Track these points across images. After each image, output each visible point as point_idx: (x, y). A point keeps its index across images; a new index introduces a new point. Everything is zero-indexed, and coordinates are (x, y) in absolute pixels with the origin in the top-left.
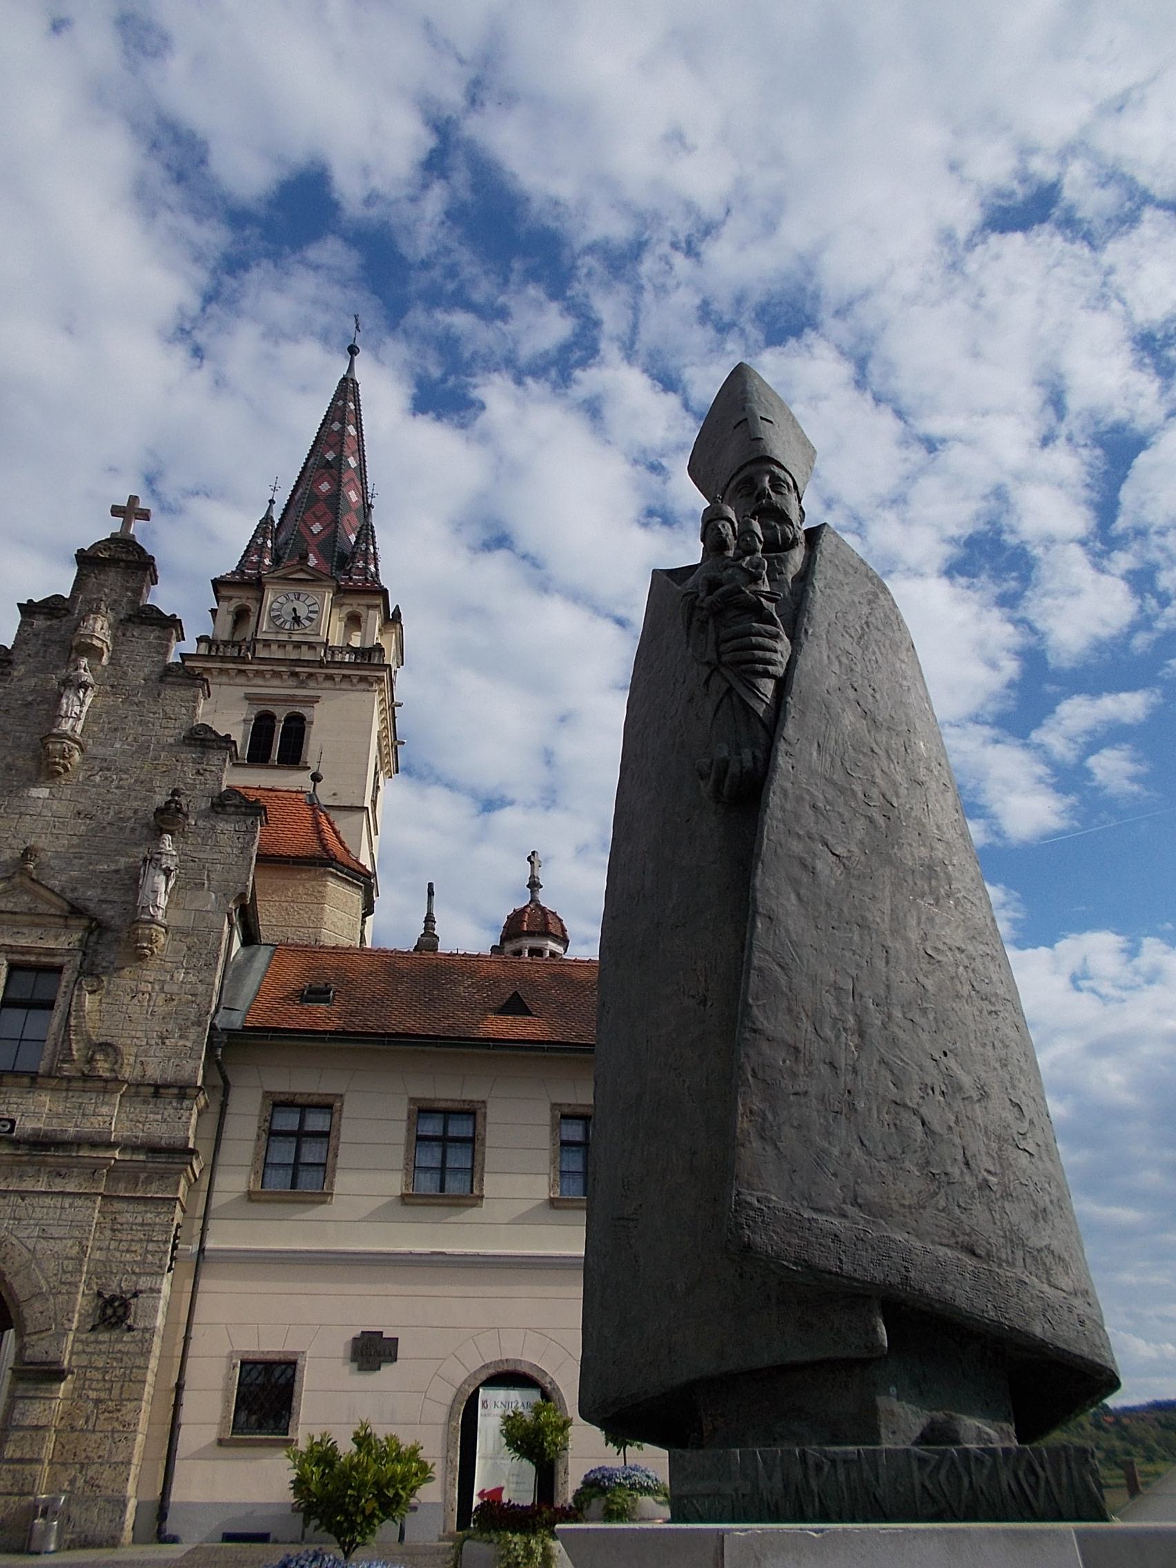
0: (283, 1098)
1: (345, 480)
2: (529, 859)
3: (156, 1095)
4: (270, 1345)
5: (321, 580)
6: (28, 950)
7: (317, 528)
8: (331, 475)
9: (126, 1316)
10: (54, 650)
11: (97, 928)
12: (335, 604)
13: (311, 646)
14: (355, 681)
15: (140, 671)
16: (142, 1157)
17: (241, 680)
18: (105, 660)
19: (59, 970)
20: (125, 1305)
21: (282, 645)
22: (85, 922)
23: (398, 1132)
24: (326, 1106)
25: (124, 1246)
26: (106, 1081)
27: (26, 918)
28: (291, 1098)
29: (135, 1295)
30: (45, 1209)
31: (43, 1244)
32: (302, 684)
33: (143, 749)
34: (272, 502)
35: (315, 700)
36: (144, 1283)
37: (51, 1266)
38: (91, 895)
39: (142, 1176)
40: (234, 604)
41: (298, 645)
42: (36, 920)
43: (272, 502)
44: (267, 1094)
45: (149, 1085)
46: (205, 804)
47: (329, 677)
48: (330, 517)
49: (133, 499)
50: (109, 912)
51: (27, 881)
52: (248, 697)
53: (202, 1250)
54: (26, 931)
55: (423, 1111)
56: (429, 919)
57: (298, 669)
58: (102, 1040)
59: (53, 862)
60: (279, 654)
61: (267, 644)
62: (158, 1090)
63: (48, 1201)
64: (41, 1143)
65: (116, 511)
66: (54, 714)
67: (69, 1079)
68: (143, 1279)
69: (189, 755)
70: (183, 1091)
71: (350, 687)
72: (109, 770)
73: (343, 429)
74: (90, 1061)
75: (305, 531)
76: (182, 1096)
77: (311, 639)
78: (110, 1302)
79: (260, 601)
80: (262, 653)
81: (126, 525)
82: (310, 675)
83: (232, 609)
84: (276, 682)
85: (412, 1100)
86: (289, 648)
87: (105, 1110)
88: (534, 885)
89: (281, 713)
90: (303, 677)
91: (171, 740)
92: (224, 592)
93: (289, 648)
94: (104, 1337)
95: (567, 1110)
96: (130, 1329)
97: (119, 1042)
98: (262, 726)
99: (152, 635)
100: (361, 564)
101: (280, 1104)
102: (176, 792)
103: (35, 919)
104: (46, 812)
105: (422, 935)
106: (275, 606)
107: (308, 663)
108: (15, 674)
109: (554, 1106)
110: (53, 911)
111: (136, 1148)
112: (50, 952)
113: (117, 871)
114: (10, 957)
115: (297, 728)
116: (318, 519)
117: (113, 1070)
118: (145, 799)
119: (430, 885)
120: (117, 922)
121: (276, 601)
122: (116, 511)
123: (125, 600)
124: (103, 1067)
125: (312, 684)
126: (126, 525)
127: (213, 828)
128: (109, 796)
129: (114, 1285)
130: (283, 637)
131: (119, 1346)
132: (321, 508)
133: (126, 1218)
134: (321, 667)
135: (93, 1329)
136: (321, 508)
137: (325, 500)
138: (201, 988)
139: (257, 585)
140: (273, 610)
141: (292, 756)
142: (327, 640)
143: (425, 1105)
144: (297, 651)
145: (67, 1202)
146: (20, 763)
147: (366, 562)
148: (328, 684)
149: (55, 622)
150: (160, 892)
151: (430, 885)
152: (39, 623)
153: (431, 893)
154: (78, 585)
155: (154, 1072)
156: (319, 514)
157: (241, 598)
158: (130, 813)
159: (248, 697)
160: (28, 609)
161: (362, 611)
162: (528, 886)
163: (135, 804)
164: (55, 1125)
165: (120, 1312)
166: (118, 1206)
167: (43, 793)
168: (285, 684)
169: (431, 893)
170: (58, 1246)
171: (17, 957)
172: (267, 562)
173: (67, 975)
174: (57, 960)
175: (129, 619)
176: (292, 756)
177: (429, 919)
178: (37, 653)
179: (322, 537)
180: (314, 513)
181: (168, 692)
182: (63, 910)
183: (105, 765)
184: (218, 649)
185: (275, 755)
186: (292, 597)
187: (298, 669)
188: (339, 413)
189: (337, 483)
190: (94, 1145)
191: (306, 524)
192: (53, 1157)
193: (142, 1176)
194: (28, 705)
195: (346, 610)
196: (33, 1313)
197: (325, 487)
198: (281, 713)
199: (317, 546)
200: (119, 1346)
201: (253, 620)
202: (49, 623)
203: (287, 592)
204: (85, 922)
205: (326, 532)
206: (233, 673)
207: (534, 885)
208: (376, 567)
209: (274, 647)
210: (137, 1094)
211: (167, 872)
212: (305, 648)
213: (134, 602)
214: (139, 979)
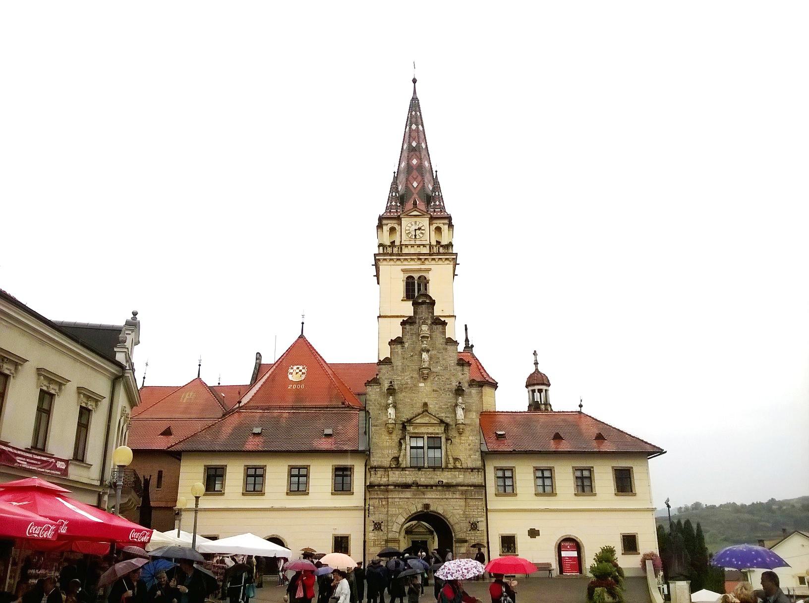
0: (499, 468)
1: (423, 156)
3: (472, 471)
4: (508, 532)
5: (425, 215)
6: (432, 434)
7: (415, 184)
8: (416, 155)
9: (477, 527)
10: (414, 337)
11: (447, 425)
13: (424, 246)
14: (444, 260)
15: (440, 341)
16: (473, 488)
17: (399, 262)
18: (429, 339)
20: (476, 524)
21: (412, 246)
22: (445, 425)
23: (532, 477)
24: (511, 470)
25: (472, 510)
26: (460, 469)
27: (430, 425)
28: (501, 468)
29: (478, 522)
30: (453, 502)
31: (454, 511)
32: (423, 263)
33: (446, 368)
34: (395, 173)
35: (428, 270)
36: (479, 519)
37: (458, 517)
38: (442, 415)
39: (473, 493)
40: (389, 226)
41: (419, 246)
42: (433, 425)
44: (495, 467)
45: (469, 469)
46: (466, 385)
47: (433, 259)
48: (419, 178)
50: (448, 420)
51: (427, 413)
52: (403, 270)
53: (487, 509)
54: (430, 428)
55: (537, 469)
57: (421, 257)
58: (455, 457)
59: (431, 406)
60: (412, 251)
61: (406, 246)
62: (472, 469)
63: (452, 500)
64: (448, 486)
66: (421, 360)
67: (451, 469)
68: (479, 518)
69: (459, 368)
70: (478, 469)
71: (442, 263)
72: (438, 375)
73: (418, 128)
75: (410, 186)
76: (478, 471)
77: (424, 243)
78: (472, 524)
80: (405, 251)
82: (426, 259)
83: (388, 229)
84: (412, 263)
85: (534, 467)
86: (416, 247)
87: (461, 476)
88: (536, 364)
89: (416, 276)
90: (423, 260)
91: (453, 364)
93: (416, 247)
94: (473, 532)
95: (577, 468)
96: (478, 530)
97: (461, 457)
99: (440, 327)
100: (437, 203)
101: (497, 469)
102: (460, 383)
103: (433, 425)
104: (425, 391)
105: (465, 348)
106: (407, 228)
107: (425, 254)
108: (406, 346)
109: (573, 467)
110: (435, 422)
111: (471, 486)
112: (438, 434)
113: (448, 408)
114: (428, 435)
116: (415, 179)
117: (461, 466)
118: (451, 384)
119: (466, 326)
120: (451, 423)
121: (407, 226)
123: (430, 317)
124: (458, 465)
125: (427, 262)
127: (470, 392)
128: (441, 384)
129: (472, 520)
130: (412, 243)
131: (477, 534)
132: (415, 173)
133: (471, 503)
134: (430, 256)
135: (470, 530)
136: (415, 173)
137: (416, 169)
138: (477, 441)
139: (399, 219)
140: (407, 230)
142: (430, 243)
143: (537, 468)
144: (419, 248)
145: (457, 500)
146: (414, 375)
147: (440, 203)
148: (433, 262)
149: (412, 327)
151: (466, 326)
152: (408, 327)
153: (466, 329)
154: (415, 312)
155: (470, 465)
156: (415, 177)
158: (447, 389)
159: (403, 270)
161: (441, 226)
162: (534, 364)
163: (448, 386)
164: (450, 481)
165: (475, 526)
166: (469, 500)
167: (422, 385)
168: (416, 264)
169: (466, 329)
170: (458, 511)
171: (430, 435)
172: (398, 204)
173: (443, 440)
174: (440, 436)
175: (433, 323)
178: (410, 339)
179: (418, 189)
180: (412, 176)
181: (449, 347)
182: (438, 421)
183: (437, 374)
184: (386, 249)
186: (413, 223)
187: (421, 257)
188: (414, 120)
189: (420, 159)
190: (462, 486)
191: (410, 182)
192: (452, 489)
193: (473, 493)
194: (412, 356)
195: (435, 226)
196: (457, 528)
197: (415, 162)
198: (416, 276)
199: (417, 194)
200: (477, 534)
201: (398, 233)
202: (411, 327)
203: (411, 221)
204: (445, 425)
205: (420, 186)
206: (395, 260)
207: (536, 364)
208: (443, 203)
209: (409, 247)
210: (467, 472)
211: (463, 409)
212: (422, 247)
213: (433, 316)
214: (461, 439)
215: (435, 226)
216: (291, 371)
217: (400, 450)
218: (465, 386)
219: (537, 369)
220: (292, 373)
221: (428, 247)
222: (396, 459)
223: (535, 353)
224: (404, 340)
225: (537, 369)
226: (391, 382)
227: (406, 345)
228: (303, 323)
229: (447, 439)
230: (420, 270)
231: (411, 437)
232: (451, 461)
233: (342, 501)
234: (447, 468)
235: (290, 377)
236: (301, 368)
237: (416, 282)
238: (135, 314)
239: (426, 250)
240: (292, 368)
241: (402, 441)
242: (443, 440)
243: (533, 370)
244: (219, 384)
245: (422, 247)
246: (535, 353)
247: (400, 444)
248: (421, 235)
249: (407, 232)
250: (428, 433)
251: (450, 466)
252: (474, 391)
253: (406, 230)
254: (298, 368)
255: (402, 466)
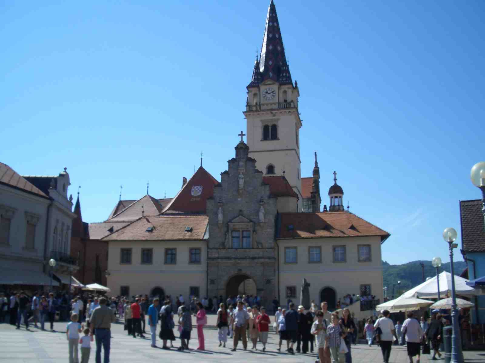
2: (334, 173)
11: (255, 223)
12: (279, 89)
13: (275, 104)
17: (258, 116)
19: (250, 231)
21: (267, 104)
34: (257, 56)
35: (278, 119)
38: (252, 217)
40: (253, 92)
41: (271, 104)
43: (257, 56)
46: (266, 198)
49: (242, 132)
50: (254, 220)
56: (316, 163)
61: (263, 105)
64: (254, 258)
65: (239, 135)
74: (258, 245)
79: (260, 91)
81: (242, 138)
88: (335, 180)
92: (250, 89)
98: (266, 129)
100: (284, 74)
107: (275, 110)
115: (275, 127)
119: (315, 153)
122: (239, 135)
126: (242, 138)
139: (258, 87)
141: (275, 137)
150: (261, 216)
151: (315, 153)
154: (237, 155)
157: (255, 90)
160: (229, 162)
161: (287, 90)
162: (334, 180)
167: (239, 199)
176: (275, 137)
177: (316, 163)
185: (270, 137)
195: (282, 90)
207: (335, 180)
212: (273, 105)
215: (282, 90)
216: (194, 189)
217: (225, 239)
218: (266, 199)
219: (336, 184)
220: (193, 191)
221: (277, 105)
222: (223, 244)
223: (335, 173)
224: (230, 172)
225: (336, 184)
226: (220, 198)
227: (231, 175)
228: (201, 159)
229: (254, 231)
230: (272, 120)
231: (232, 231)
232: (256, 244)
233: (195, 267)
234: (253, 248)
235: (192, 194)
236: (199, 187)
237: (270, 128)
238: (65, 169)
239: (276, 107)
240: (194, 188)
241: (227, 234)
242: (252, 232)
243: (332, 184)
244: (165, 197)
245: (273, 105)
246: (335, 173)
247: (226, 235)
248: (273, 97)
249: (264, 95)
250: (242, 228)
251: (255, 247)
252: (271, 201)
253: (263, 94)
254: (197, 188)
255: (227, 247)
